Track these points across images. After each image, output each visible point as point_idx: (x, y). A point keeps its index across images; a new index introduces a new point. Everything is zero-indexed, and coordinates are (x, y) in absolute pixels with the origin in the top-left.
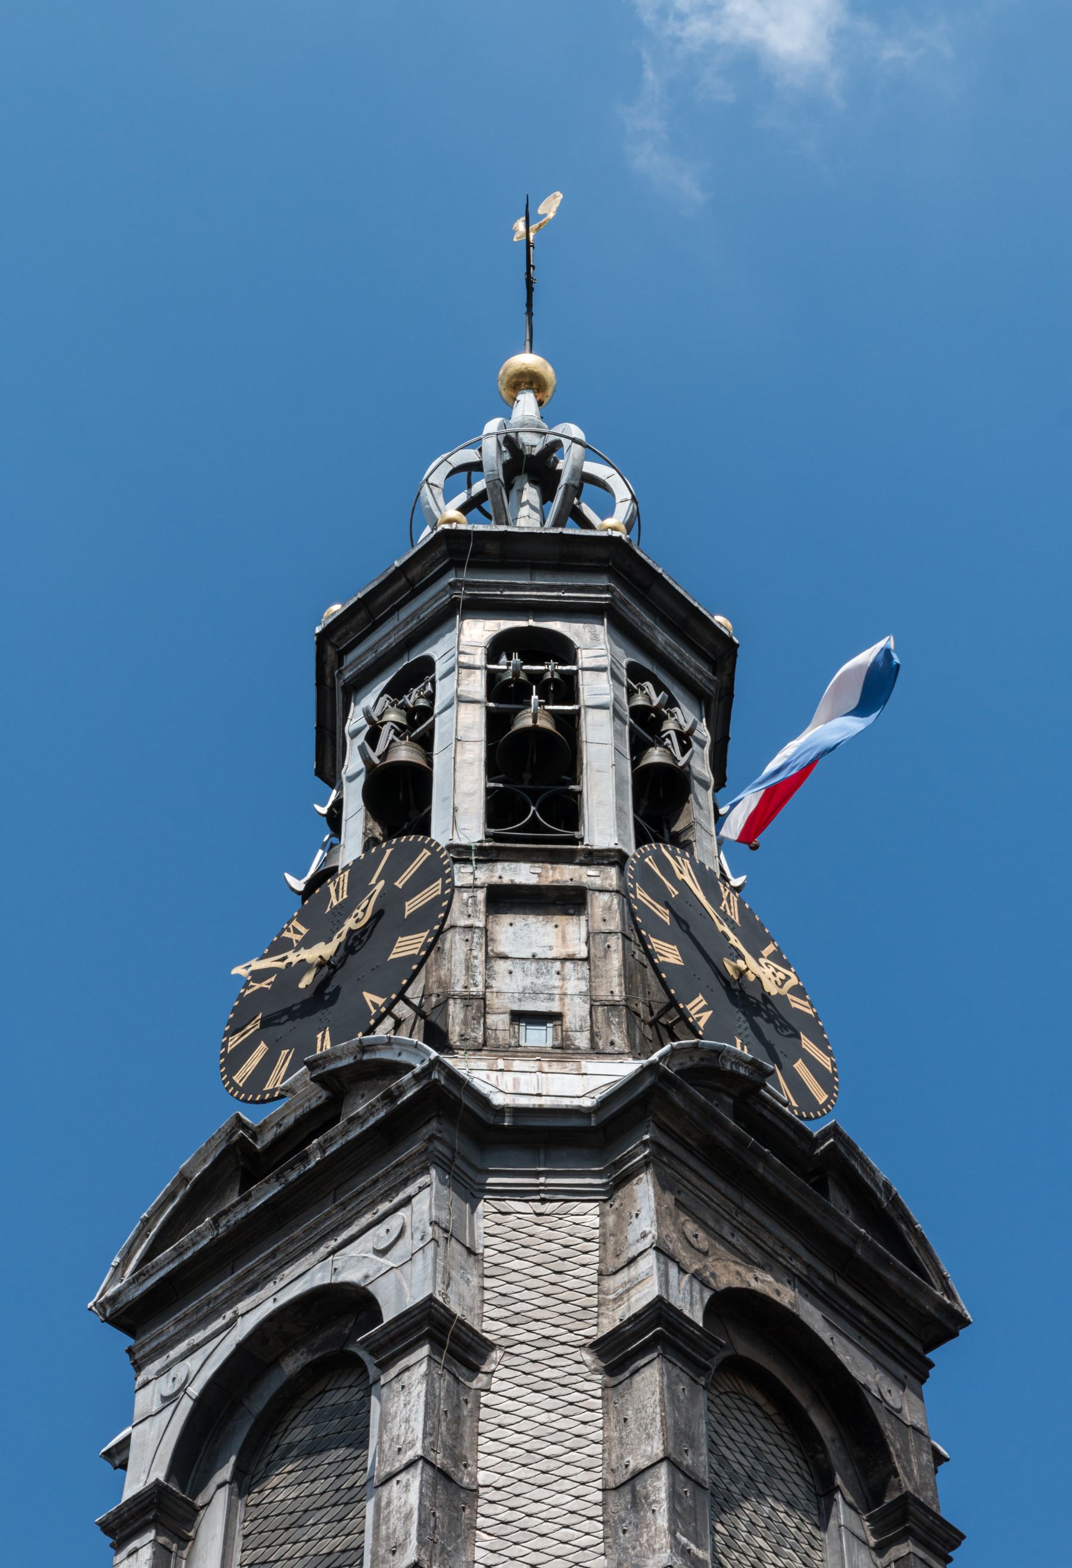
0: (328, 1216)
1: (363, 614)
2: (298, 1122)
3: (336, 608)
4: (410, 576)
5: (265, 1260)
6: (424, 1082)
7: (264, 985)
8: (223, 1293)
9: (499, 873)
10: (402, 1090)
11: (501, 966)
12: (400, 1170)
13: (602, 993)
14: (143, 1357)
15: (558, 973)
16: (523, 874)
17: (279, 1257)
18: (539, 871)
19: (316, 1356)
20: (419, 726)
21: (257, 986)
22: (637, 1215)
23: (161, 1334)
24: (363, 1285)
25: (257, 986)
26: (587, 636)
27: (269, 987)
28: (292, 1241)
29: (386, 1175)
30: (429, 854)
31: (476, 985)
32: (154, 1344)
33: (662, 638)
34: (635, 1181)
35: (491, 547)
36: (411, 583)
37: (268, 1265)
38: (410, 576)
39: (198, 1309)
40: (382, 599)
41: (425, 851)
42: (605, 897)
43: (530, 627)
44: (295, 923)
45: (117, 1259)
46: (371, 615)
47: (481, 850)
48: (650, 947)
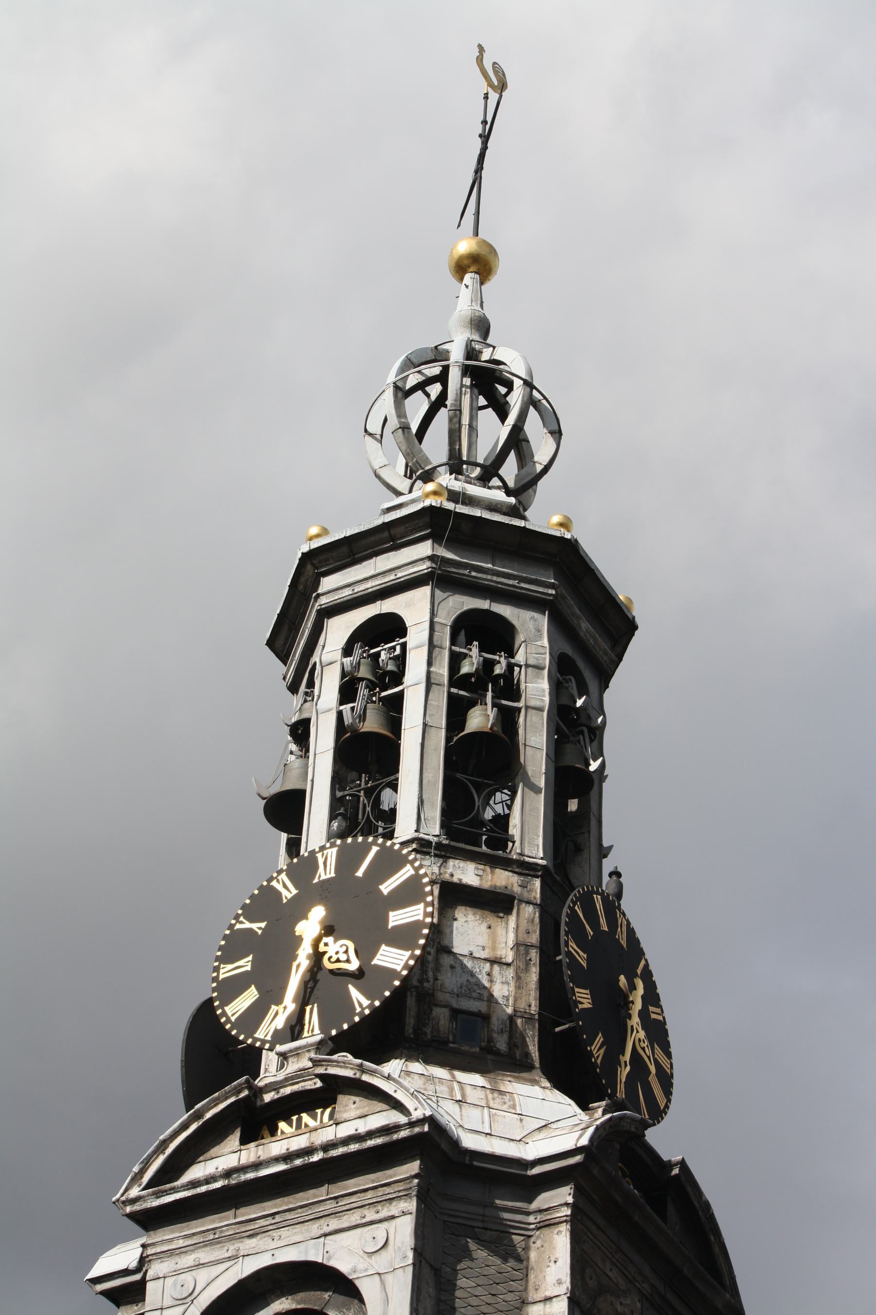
1: (345, 549)
4: (393, 532)
7: (255, 926)
9: (449, 871)
15: (488, 975)
16: (467, 873)
19: (299, 1307)
21: (247, 925)
22: (555, 1262)
23: (171, 1240)
24: (351, 1278)
25: (247, 925)
26: (531, 626)
27: (260, 932)
30: (412, 872)
31: (428, 982)
32: (165, 1248)
33: (585, 626)
34: (555, 1232)
38: (393, 532)
40: (364, 542)
41: (408, 866)
42: (530, 908)
43: (488, 612)
44: (283, 876)
45: (136, 1169)
47: (439, 845)
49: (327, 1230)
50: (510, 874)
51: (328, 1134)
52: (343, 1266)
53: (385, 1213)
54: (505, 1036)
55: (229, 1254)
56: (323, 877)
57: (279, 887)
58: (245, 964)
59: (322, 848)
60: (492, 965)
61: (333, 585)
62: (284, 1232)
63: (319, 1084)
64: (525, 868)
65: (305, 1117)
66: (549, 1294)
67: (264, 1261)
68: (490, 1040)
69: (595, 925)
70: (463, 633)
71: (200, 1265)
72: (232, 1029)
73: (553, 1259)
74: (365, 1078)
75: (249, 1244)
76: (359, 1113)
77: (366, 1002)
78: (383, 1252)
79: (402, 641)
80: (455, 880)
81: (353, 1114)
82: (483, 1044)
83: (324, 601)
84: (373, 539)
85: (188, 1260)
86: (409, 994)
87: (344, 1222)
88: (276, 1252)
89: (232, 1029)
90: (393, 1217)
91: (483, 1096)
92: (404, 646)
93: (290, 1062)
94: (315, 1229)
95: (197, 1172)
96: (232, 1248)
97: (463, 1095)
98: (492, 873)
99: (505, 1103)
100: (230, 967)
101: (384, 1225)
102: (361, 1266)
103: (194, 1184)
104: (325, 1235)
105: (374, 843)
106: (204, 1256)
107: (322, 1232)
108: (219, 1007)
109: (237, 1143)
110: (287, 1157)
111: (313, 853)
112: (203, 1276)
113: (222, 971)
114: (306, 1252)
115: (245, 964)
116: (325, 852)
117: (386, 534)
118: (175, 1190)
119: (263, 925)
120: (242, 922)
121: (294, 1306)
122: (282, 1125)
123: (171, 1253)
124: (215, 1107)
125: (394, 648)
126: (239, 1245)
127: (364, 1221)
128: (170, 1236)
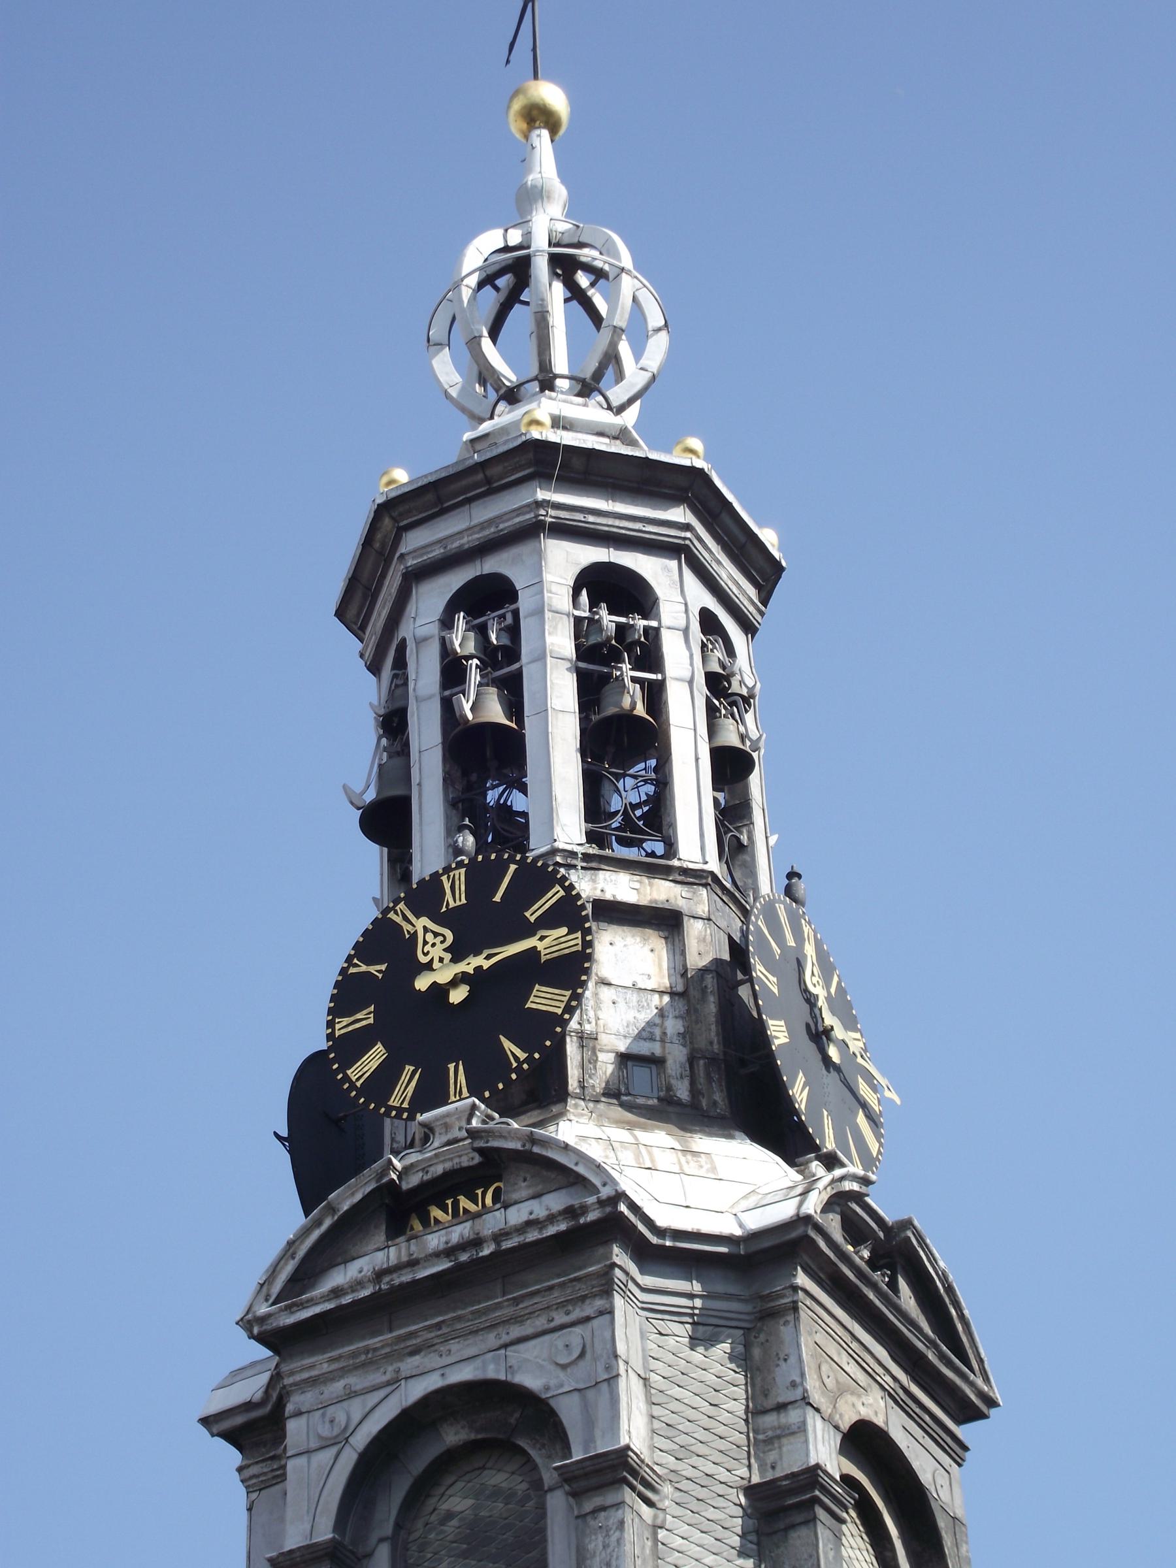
0: (498, 1306)
1: (430, 497)
2: (446, 1175)
3: (401, 476)
4: (489, 473)
5: (429, 1328)
6: (608, 1209)
7: (372, 969)
8: (383, 1347)
9: (600, 887)
10: (584, 1209)
11: (606, 993)
12: (578, 1286)
13: (702, 1043)
14: (295, 1384)
17: (445, 1330)
18: (637, 885)
19: (479, 1436)
20: (505, 667)
22: (785, 1360)
23: (312, 1367)
24: (544, 1396)
27: (380, 976)
28: (459, 1319)
29: (562, 1285)
30: (562, 893)
32: (305, 1375)
34: (782, 1322)
35: (577, 463)
36: (488, 481)
37: (433, 1335)
38: (489, 473)
39: (354, 1355)
41: (557, 888)
46: (440, 500)
47: (587, 857)
48: (744, 992)
49: (505, 1339)
50: (672, 884)
51: (494, 1222)
52: (531, 1381)
53: (577, 1314)
54: (686, 1082)
55: (388, 1377)
56: (452, 904)
57: (399, 919)
58: (365, 1017)
59: (447, 870)
60: (661, 997)
61: (420, 542)
62: (454, 1346)
63: (477, 1159)
64: (693, 877)
65: (464, 1203)
66: (781, 1399)
67: (433, 1382)
68: (669, 1088)
69: (781, 941)
70: (584, 592)
71: (351, 1394)
72: (357, 1097)
73: (782, 1356)
74: (536, 1150)
75: (410, 1364)
76: (531, 1192)
77: (523, 1056)
78: (581, 1363)
79: (513, 607)
80: (608, 896)
81: (524, 1193)
82: (662, 1094)
83: (411, 562)
84: (464, 483)
85: (338, 1387)
86: (568, 1039)
87: (528, 1329)
88: (447, 1370)
89: (357, 1097)
90: (588, 1319)
91: (676, 1161)
92: (516, 614)
93: (437, 1135)
94: (491, 1339)
95: (338, 1278)
96: (390, 1369)
97: (652, 1161)
98: (650, 885)
99: (701, 1167)
100: (346, 1021)
101: (577, 1330)
102: (553, 1383)
103: (337, 1292)
104: (505, 1346)
105: (512, 860)
106: (356, 1381)
107: (502, 1342)
108: (338, 1071)
109: (383, 1237)
110: (449, 1252)
111: (436, 876)
112: (356, 1408)
113: (338, 1026)
114: (484, 1367)
115: (365, 1017)
116: (451, 874)
117: (480, 476)
118: (312, 1302)
119: (383, 967)
120: (356, 965)
121: (473, 1436)
122: (436, 1212)
123: (314, 1382)
124: (347, 1197)
125: (503, 616)
126: (400, 1364)
127: (552, 1325)
128: (319, 1363)
